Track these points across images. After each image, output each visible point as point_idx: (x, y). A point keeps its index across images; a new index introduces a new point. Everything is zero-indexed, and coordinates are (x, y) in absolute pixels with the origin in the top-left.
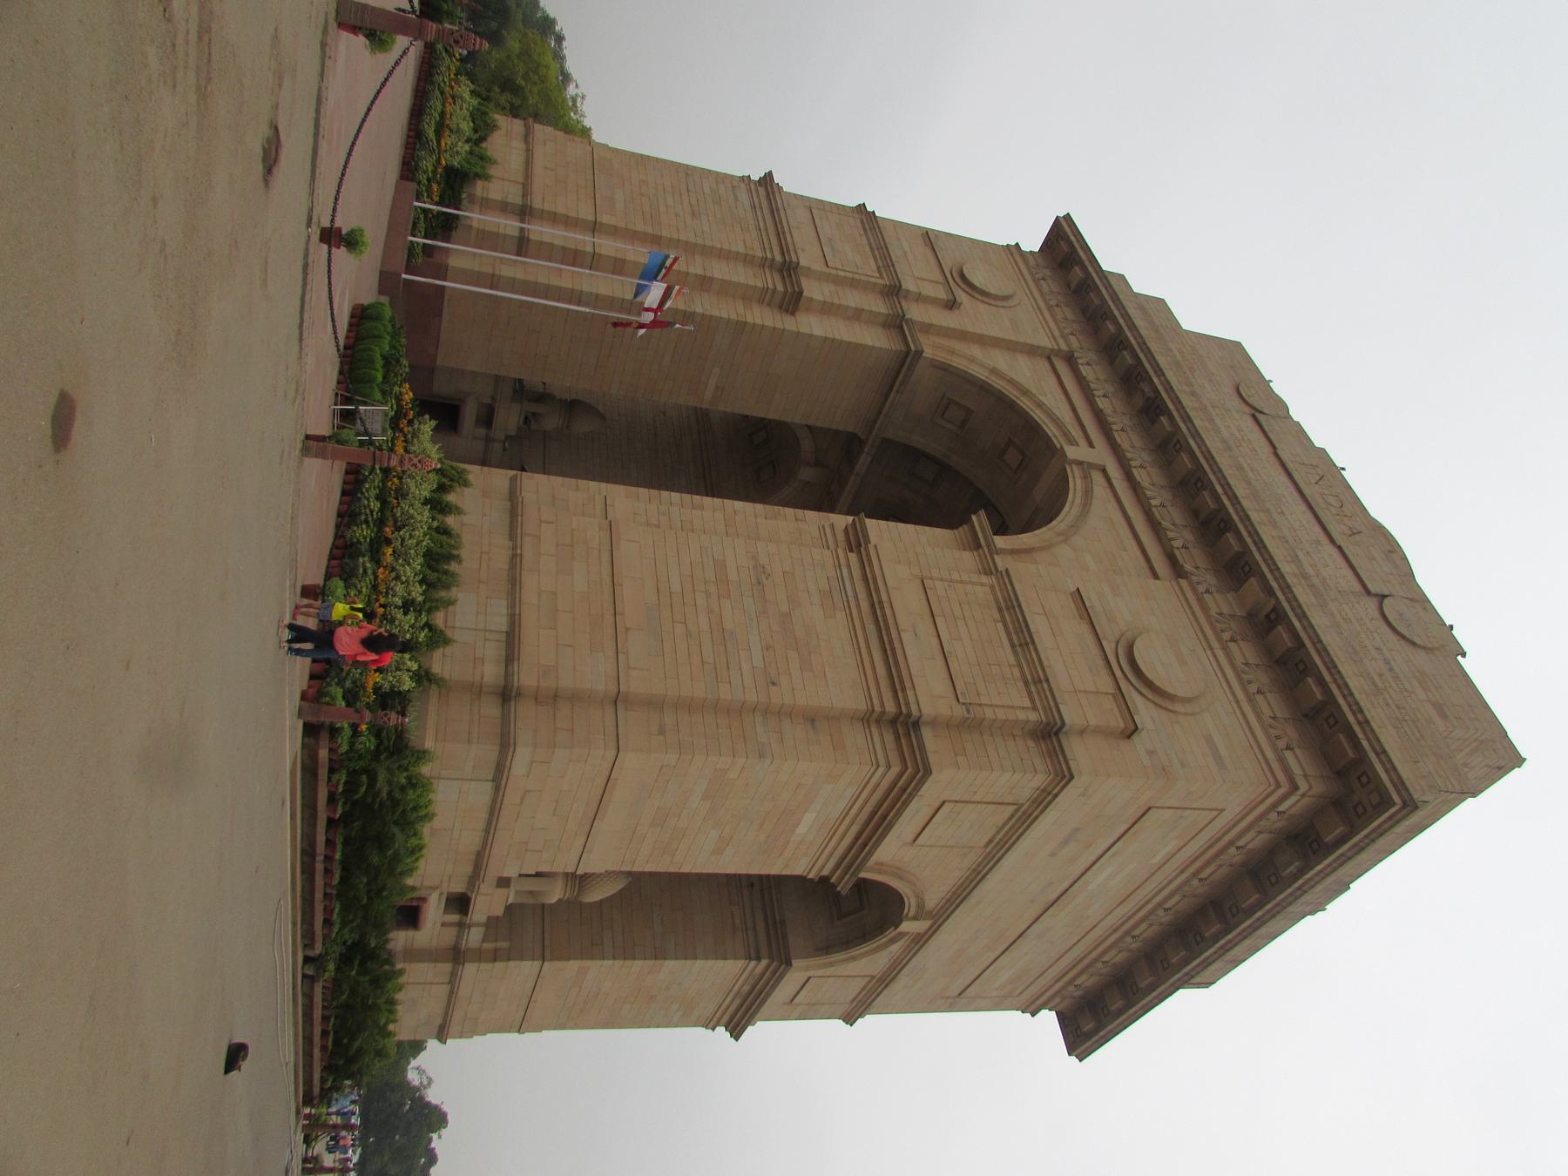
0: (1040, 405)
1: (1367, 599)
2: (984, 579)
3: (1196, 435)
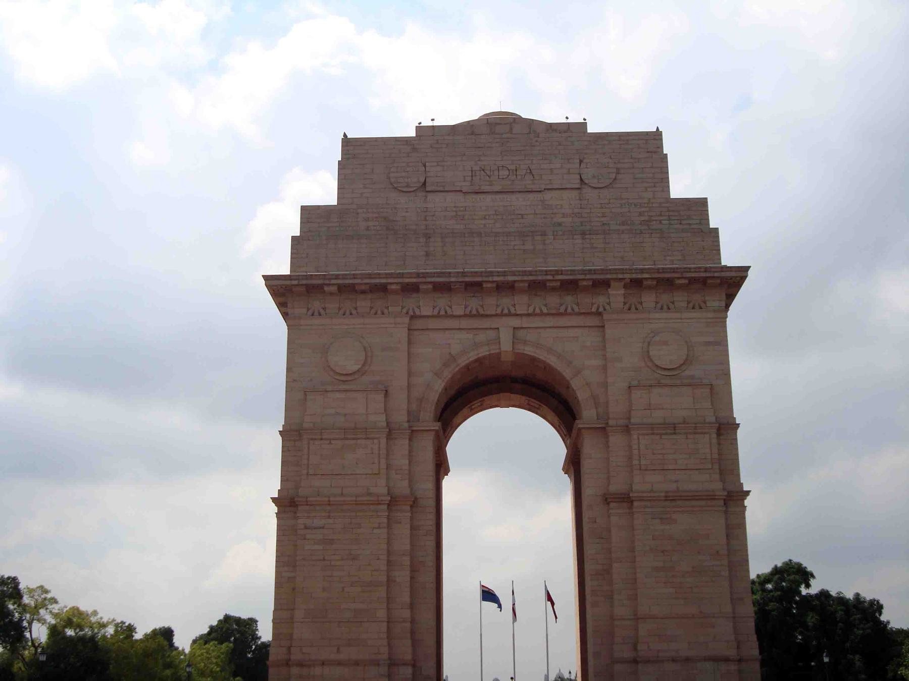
1: (584, 191)
3: (504, 274)
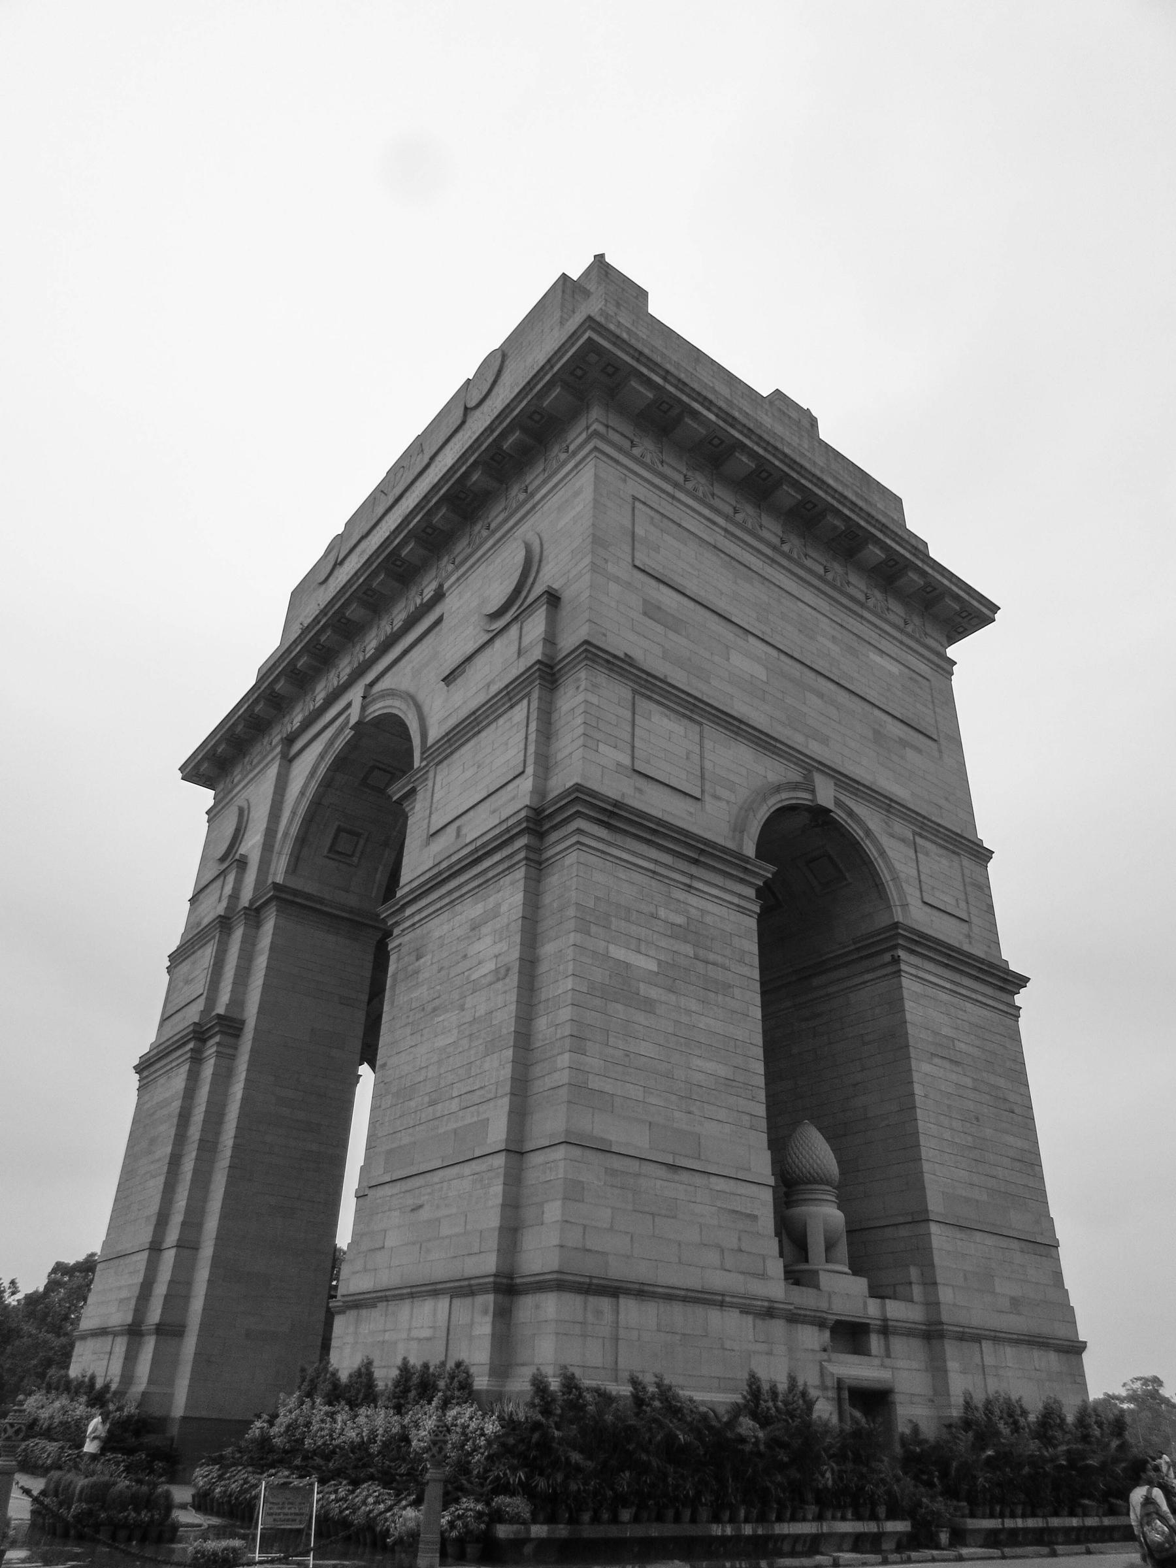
0: (322, 756)
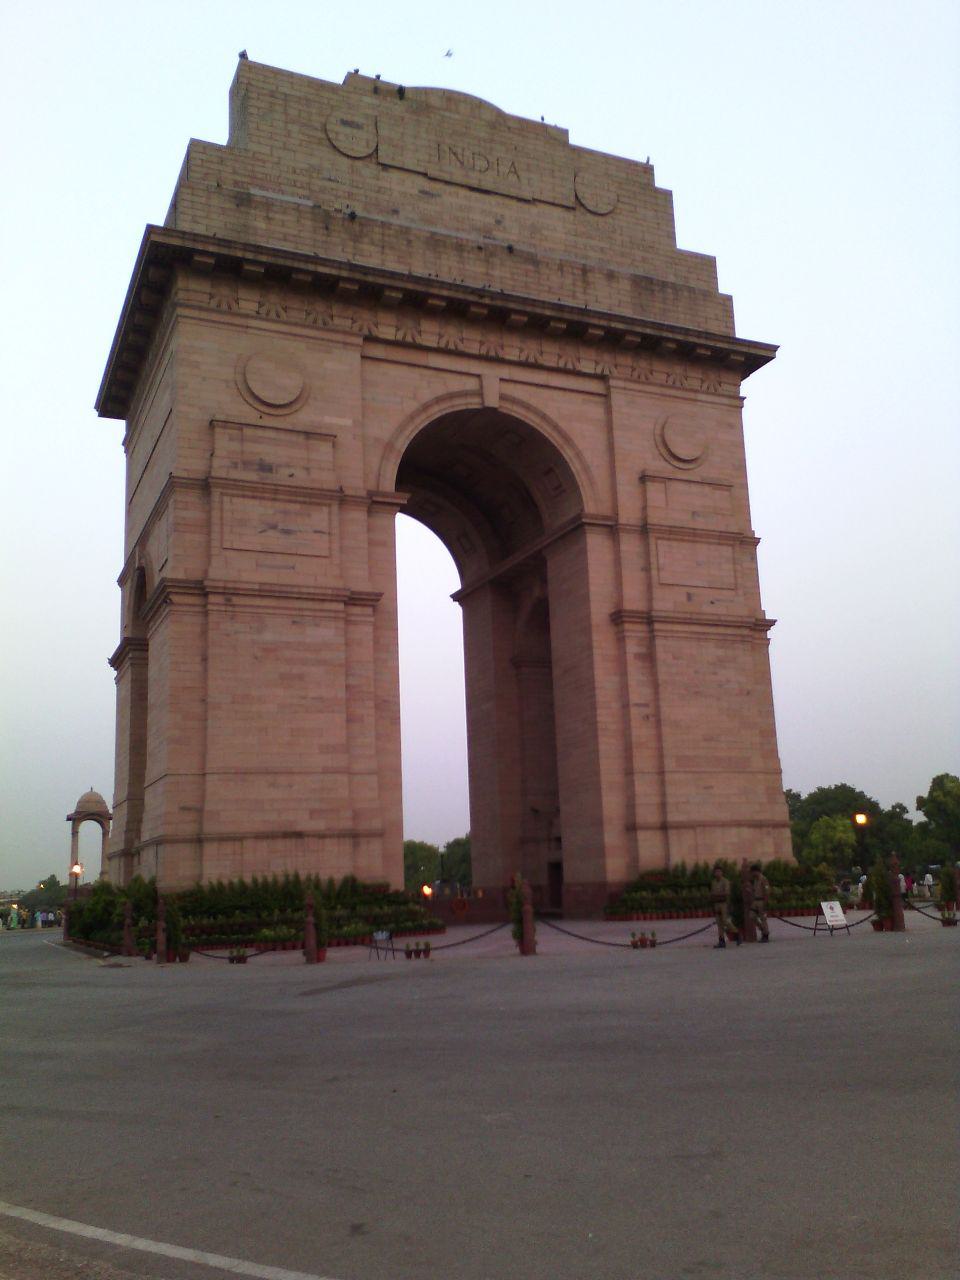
2: (652, 541)
